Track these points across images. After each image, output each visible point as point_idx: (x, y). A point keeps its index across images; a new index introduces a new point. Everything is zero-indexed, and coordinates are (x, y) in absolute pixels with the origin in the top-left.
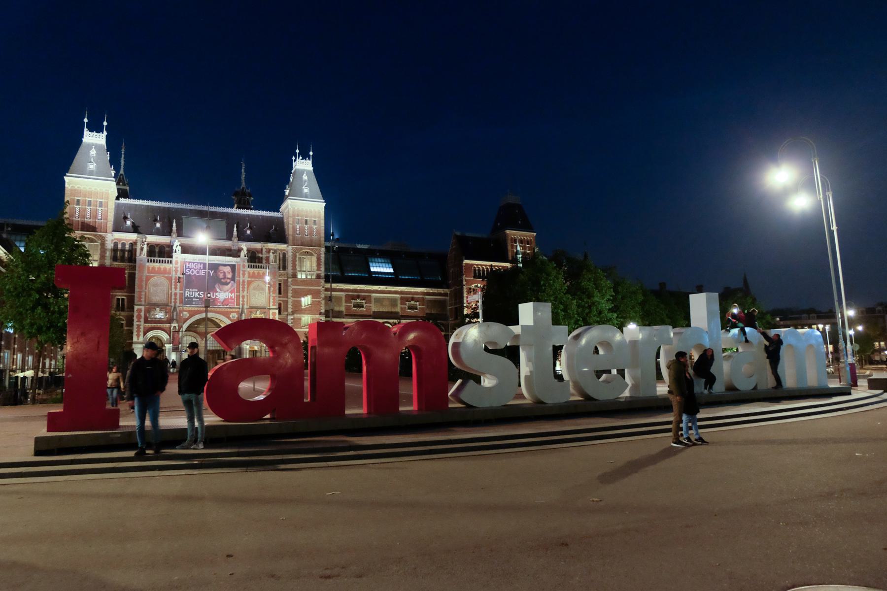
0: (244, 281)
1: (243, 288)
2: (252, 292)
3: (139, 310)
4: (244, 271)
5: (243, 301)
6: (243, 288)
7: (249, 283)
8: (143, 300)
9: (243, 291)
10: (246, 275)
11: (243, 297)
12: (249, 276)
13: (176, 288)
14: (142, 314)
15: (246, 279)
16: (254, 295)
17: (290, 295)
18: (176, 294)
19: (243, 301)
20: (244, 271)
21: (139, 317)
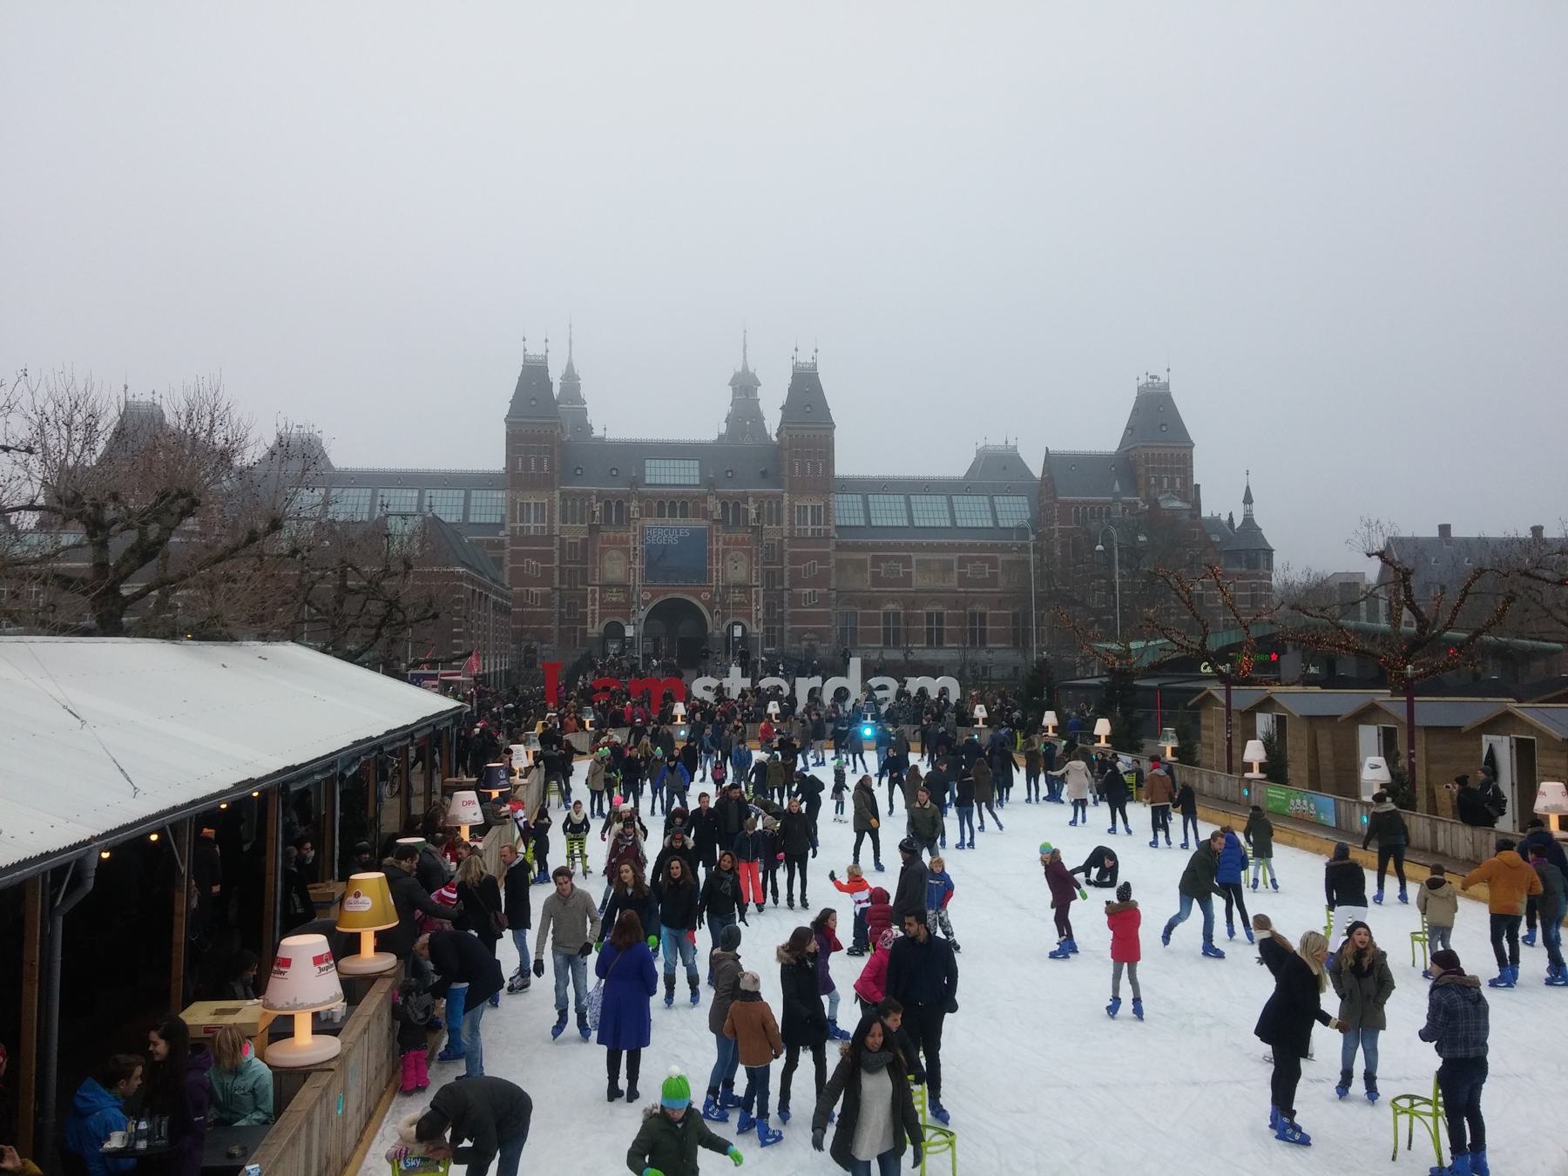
3: (593, 592)
7: (725, 552)
17: (786, 560)
21: (593, 600)
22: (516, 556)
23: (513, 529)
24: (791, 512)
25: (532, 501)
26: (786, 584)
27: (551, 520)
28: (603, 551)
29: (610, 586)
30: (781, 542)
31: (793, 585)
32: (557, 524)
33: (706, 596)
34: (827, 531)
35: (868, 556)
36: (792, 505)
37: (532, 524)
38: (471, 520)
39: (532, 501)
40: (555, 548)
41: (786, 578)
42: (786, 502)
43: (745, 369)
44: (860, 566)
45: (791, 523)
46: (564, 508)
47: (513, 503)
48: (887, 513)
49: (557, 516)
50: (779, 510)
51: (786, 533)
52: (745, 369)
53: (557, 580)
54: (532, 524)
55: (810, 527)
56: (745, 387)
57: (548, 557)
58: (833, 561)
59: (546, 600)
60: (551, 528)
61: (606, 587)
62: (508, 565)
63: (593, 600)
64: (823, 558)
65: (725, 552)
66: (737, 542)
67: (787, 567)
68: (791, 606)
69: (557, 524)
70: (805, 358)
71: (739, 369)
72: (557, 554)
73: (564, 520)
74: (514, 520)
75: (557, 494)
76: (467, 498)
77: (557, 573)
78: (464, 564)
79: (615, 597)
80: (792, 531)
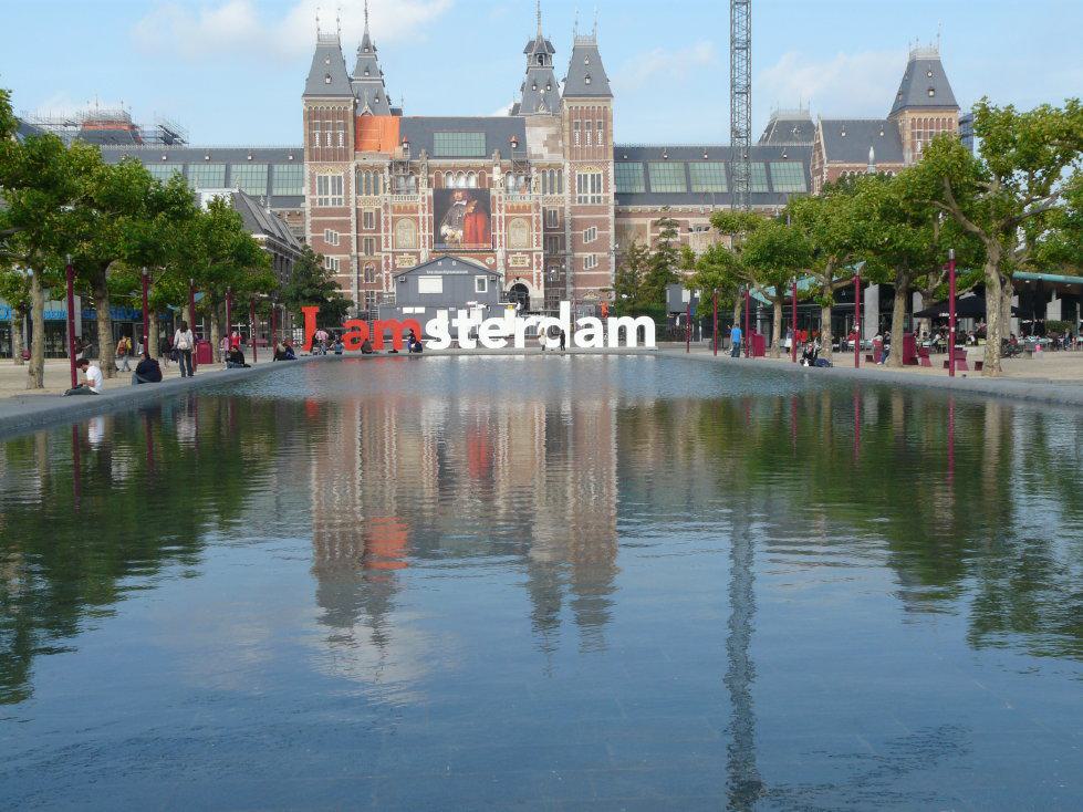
0: (500, 217)
1: (501, 226)
2: (512, 230)
3: (387, 258)
4: (500, 205)
5: (501, 242)
6: (501, 226)
7: (508, 220)
8: (390, 245)
9: (501, 229)
10: (503, 211)
11: (501, 236)
12: (507, 211)
13: (424, 230)
14: (390, 261)
15: (503, 214)
16: (514, 235)
18: (424, 237)
19: (501, 242)
20: (500, 205)
22: (317, 227)
23: (313, 202)
24: (572, 180)
25: (330, 175)
27: (348, 192)
28: (395, 221)
29: (402, 253)
30: (562, 209)
31: (573, 250)
34: (606, 199)
35: (648, 222)
36: (572, 173)
38: (275, 193)
39: (330, 175)
41: (568, 243)
42: (567, 172)
43: (540, 37)
44: (641, 231)
45: (573, 191)
46: (358, 181)
47: (312, 176)
48: (666, 179)
49: (353, 188)
50: (560, 179)
51: (567, 200)
52: (540, 37)
53: (354, 248)
54: (330, 196)
55: (590, 195)
56: (541, 53)
57: (345, 226)
58: (612, 227)
59: (345, 266)
60: (348, 201)
63: (387, 265)
64: (603, 225)
65: (508, 220)
66: (518, 210)
67: (568, 233)
69: (353, 195)
70: (585, 31)
71: (534, 37)
72: (354, 223)
73: (358, 192)
74: (313, 192)
76: (270, 172)
78: (266, 232)
80: (573, 200)
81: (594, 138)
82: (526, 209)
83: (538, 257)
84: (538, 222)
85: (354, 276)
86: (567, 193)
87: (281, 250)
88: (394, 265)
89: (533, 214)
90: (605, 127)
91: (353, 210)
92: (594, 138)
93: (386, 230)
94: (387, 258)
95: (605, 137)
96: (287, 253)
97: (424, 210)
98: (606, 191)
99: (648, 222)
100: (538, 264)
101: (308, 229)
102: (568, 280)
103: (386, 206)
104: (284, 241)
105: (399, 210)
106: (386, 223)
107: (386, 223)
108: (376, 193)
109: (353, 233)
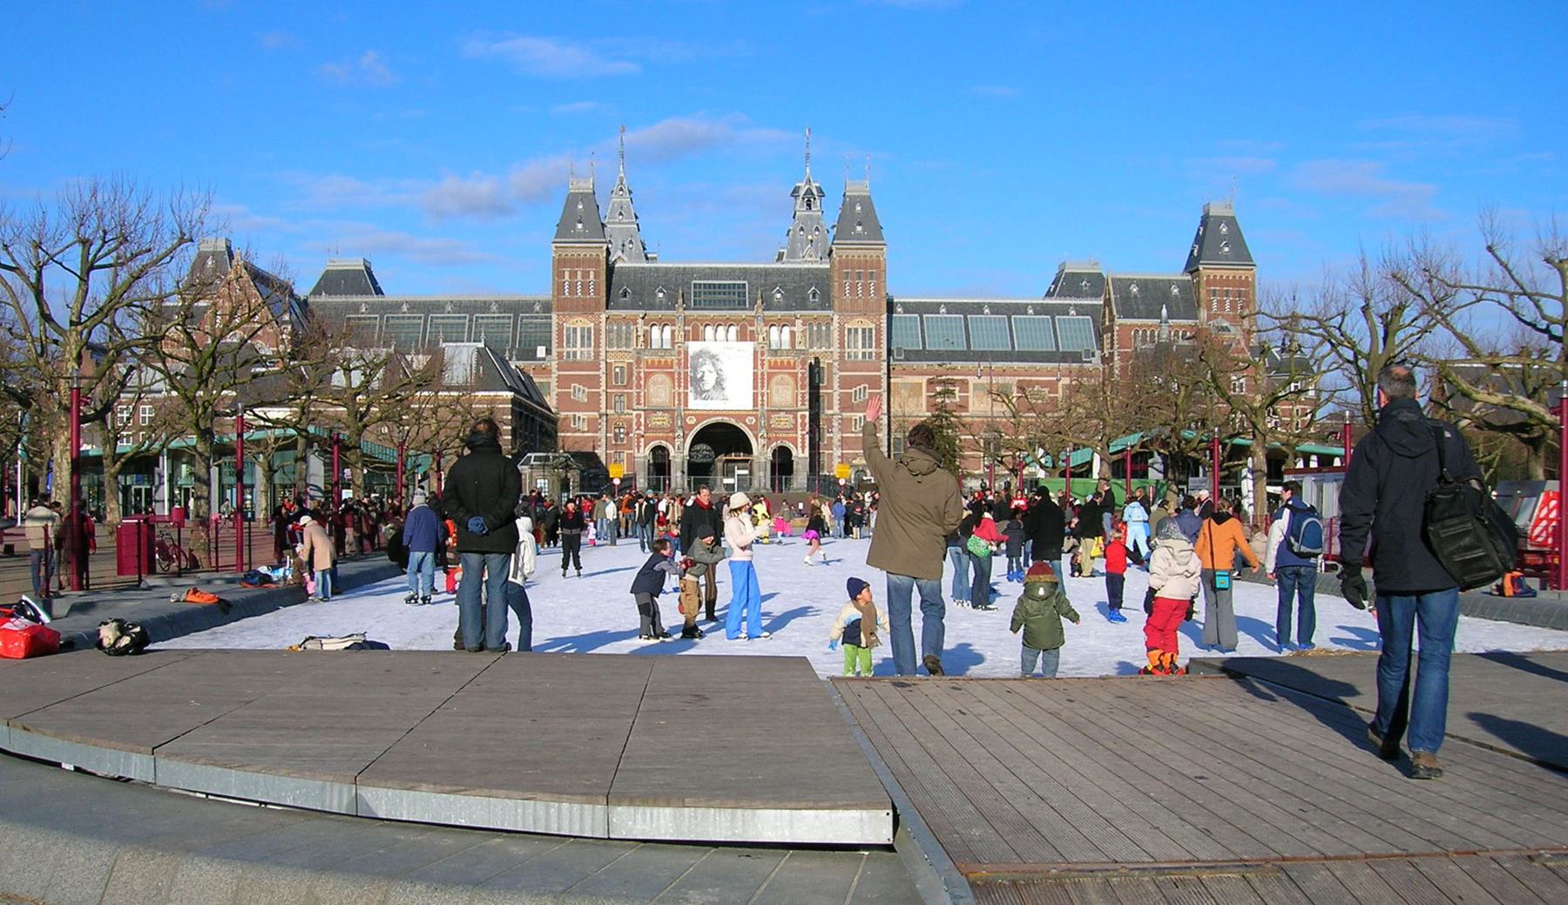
2: (774, 388)
3: (638, 416)
7: (770, 376)
23: (560, 355)
25: (579, 327)
26: (836, 408)
27: (597, 345)
28: (647, 375)
31: (842, 409)
32: (603, 350)
33: (751, 420)
37: (578, 349)
39: (579, 327)
40: (602, 373)
42: (835, 325)
45: (842, 345)
46: (608, 332)
51: (836, 356)
53: (603, 406)
54: (578, 349)
55: (860, 350)
57: (593, 382)
60: (597, 354)
61: (650, 411)
62: (554, 391)
66: (782, 366)
68: (841, 430)
72: (603, 379)
73: (609, 343)
75: (603, 317)
77: (603, 398)
78: (510, 389)
79: (660, 420)
81: (866, 288)
82: (789, 366)
83: (803, 417)
84: (803, 379)
85: (602, 434)
86: (835, 349)
87: (526, 407)
88: (646, 425)
89: (798, 370)
90: (878, 277)
91: (603, 365)
92: (866, 288)
93: (639, 386)
94: (638, 416)
95: (877, 290)
96: (532, 410)
97: (679, 365)
98: (878, 345)
99: (924, 380)
100: (803, 425)
101: (554, 384)
102: (836, 441)
103: (638, 361)
104: (530, 397)
105: (652, 365)
106: (639, 378)
107: (639, 378)
108: (627, 346)
109: (603, 387)
